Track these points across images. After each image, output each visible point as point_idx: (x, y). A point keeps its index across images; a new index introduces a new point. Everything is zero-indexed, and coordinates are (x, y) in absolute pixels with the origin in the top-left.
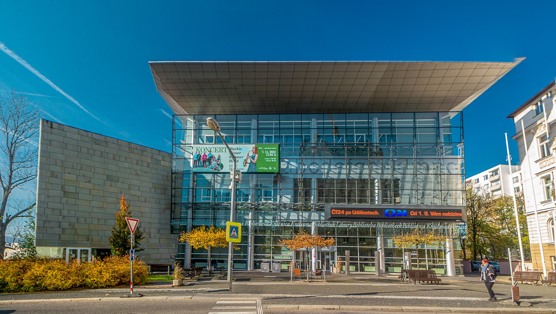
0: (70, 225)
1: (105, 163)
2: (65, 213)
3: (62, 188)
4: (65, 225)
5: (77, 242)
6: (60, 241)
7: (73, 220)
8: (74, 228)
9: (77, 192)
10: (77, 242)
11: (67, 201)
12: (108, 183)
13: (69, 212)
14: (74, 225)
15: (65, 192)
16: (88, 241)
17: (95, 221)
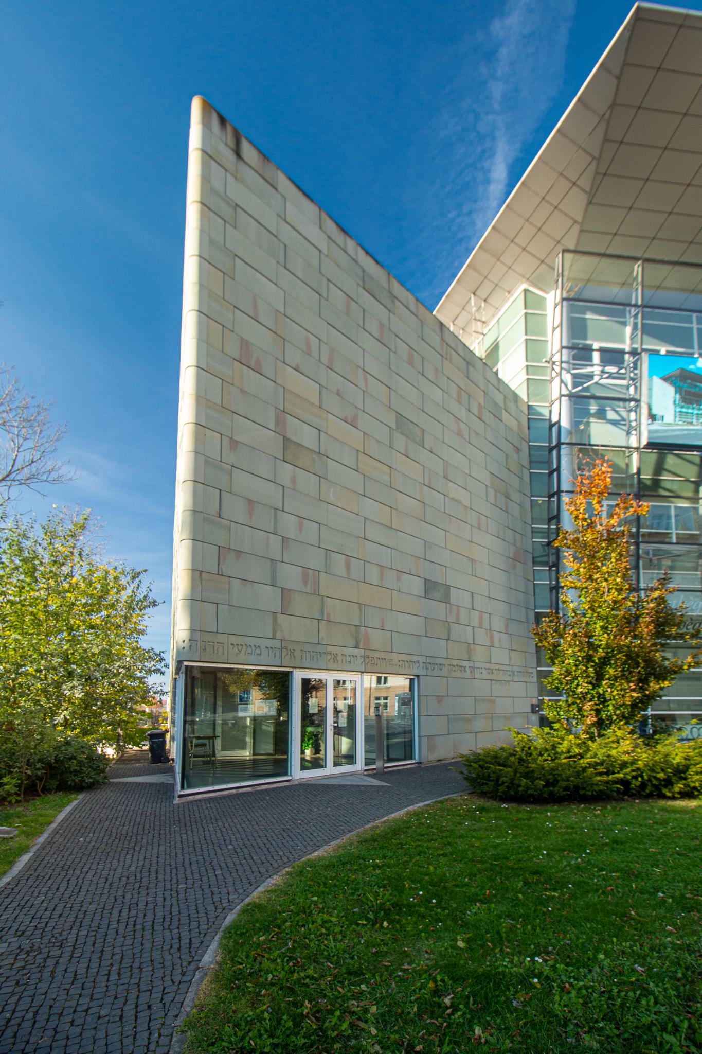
0: (305, 578)
1: (392, 367)
2: (289, 525)
3: (277, 423)
4: (291, 577)
5: (330, 648)
6: (277, 644)
7: (315, 560)
8: (316, 593)
9: (322, 451)
10: (330, 648)
11: (294, 480)
12: (400, 442)
13: (301, 527)
14: (317, 583)
15: (286, 440)
16: (357, 647)
17: (373, 576)
